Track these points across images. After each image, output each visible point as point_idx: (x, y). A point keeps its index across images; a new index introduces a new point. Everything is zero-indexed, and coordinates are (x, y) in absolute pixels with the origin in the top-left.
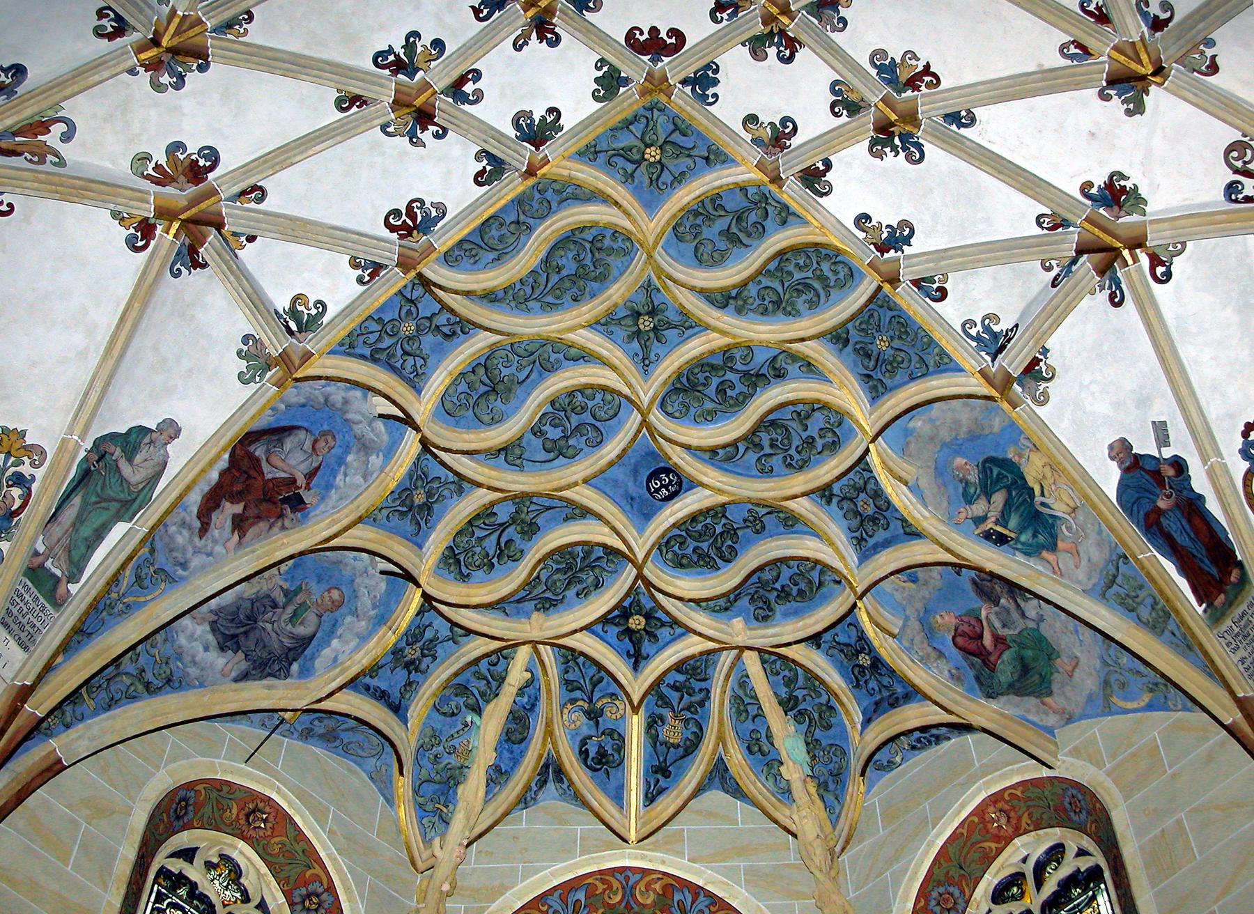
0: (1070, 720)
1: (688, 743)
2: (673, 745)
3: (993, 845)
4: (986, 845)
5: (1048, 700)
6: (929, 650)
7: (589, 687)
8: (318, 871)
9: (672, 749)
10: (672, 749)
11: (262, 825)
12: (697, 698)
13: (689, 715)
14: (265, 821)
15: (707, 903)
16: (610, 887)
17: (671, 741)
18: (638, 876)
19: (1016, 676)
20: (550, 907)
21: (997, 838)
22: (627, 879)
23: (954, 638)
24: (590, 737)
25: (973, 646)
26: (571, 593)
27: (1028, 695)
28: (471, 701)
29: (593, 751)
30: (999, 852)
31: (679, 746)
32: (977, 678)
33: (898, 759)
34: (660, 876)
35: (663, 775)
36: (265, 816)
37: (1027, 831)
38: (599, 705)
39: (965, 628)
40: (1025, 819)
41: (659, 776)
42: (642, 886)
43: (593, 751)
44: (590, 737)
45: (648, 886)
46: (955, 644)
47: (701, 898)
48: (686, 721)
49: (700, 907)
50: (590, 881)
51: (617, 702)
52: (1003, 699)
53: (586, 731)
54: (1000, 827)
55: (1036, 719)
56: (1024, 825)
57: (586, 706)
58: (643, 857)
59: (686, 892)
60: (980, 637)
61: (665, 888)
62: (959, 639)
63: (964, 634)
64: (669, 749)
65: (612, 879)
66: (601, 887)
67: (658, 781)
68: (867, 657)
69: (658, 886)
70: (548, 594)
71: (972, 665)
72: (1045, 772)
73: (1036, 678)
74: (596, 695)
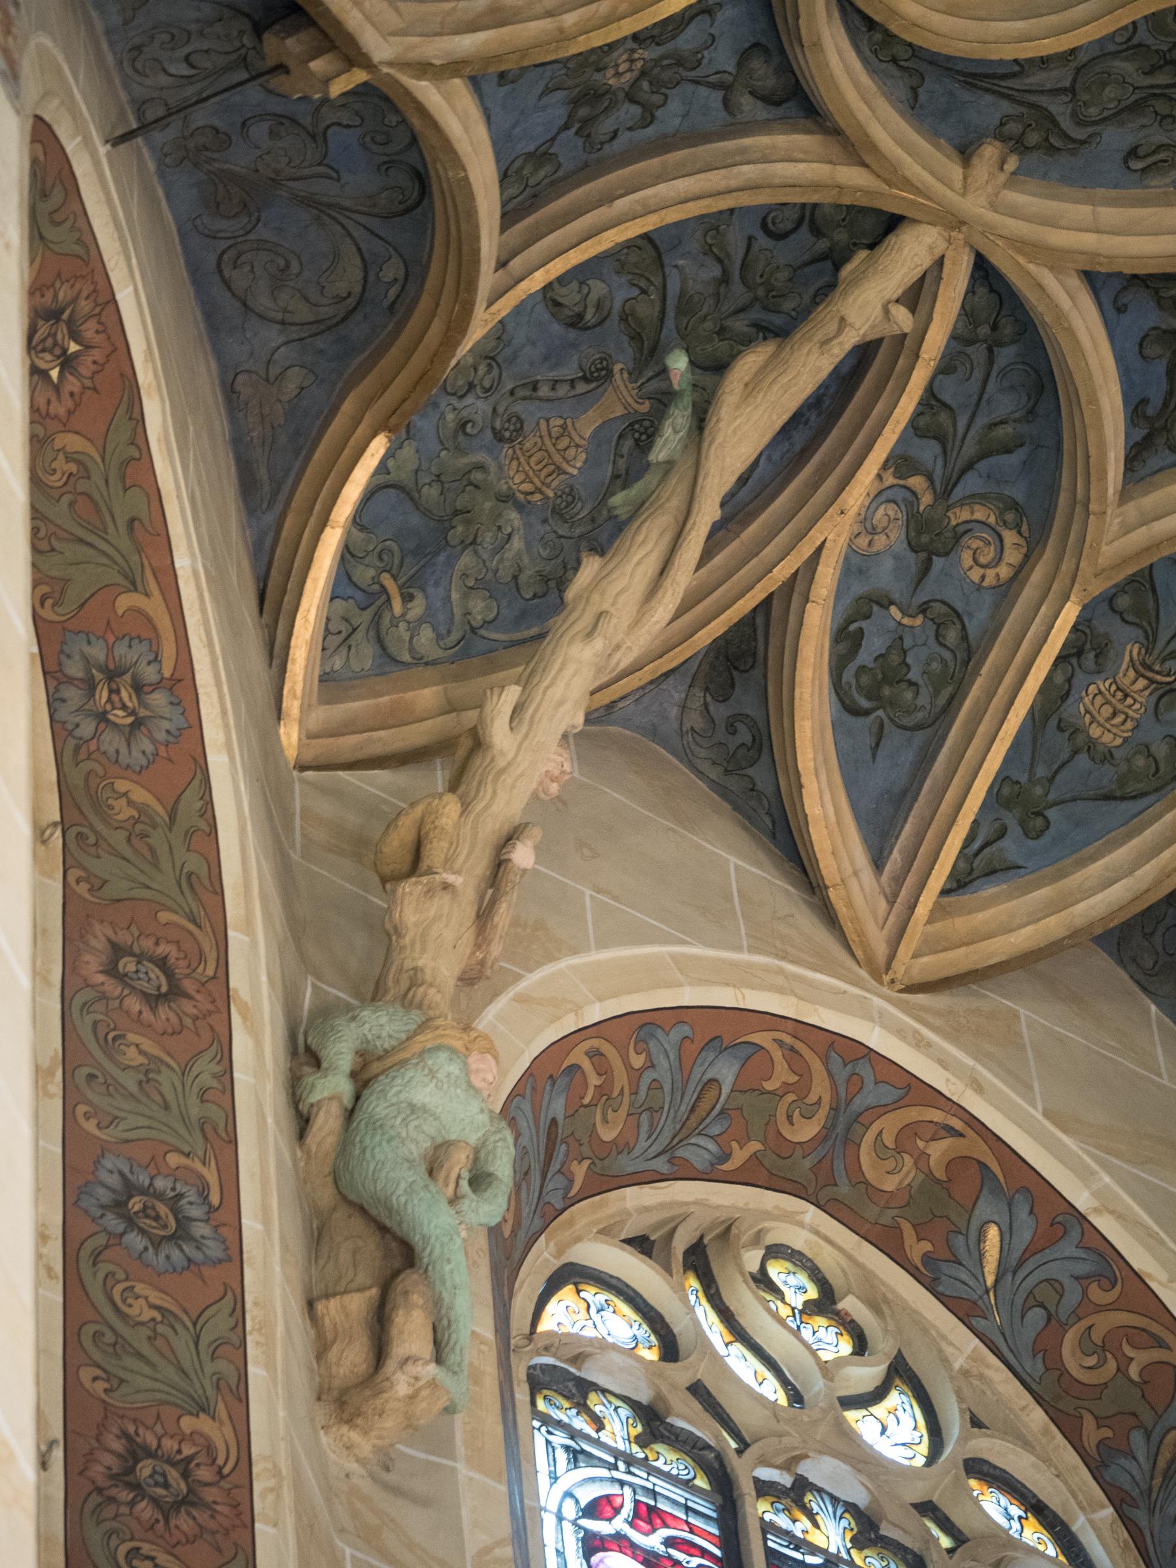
1: (1140, 761)
2: (1091, 746)
7: (970, 449)
8: (155, 606)
9: (1083, 760)
10: (1083, 760)
11: (54, 374)
15: (1082, 1268)
16: (802, 1087)
17: (1095, 731)
18: (887, 1094)
20: (651, 1065)
22: (855, 1083)
24: (885, 602)
26: (1116, 138)
28: (647, 310)
29: (874, 645)
31: (1108, 756)
35: (1022, 823)
36: (73, 347)
38: (961, 515)
41: (1011, 820)
42: (888, 1126)
43: (874, 645)
44: (885, 602)
45: (908, 1132)
47: (1068, 1248)
49: (1054, 1270)
51: (1010, 537)
53: (885, 577)
57: (926, 499)
58: (920, 1044)
59: (1023, 1212)
61: (955, 1164)
64: (1076, 752)
65: (817, 1065)
66: (782, 1075)
67: (1002, 833)
69: (938, 1151)
70: (1059, 108)
74: (971, 483)
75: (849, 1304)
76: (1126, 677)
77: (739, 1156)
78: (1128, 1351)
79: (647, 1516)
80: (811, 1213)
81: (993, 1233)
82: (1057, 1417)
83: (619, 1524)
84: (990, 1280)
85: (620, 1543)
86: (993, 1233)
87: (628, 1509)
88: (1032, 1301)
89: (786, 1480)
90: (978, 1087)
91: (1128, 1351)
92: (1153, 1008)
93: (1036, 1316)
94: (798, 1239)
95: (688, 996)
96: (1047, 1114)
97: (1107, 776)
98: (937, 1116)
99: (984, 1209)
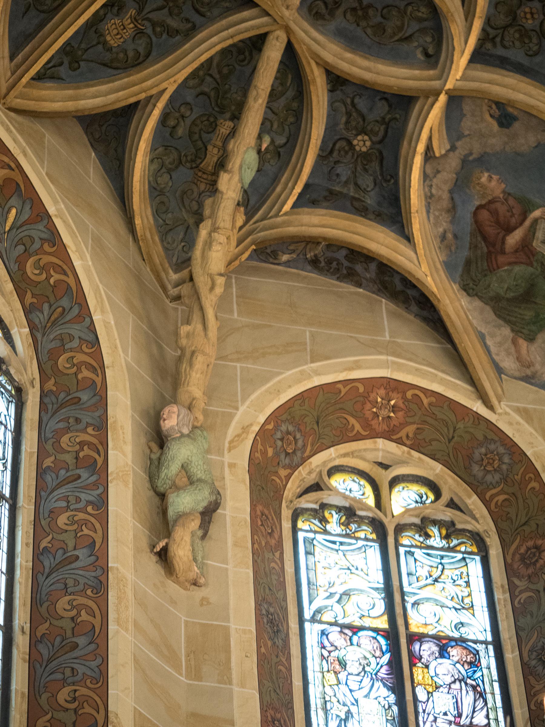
0: (528, 379)
1: (121, 55)
2: (105, 43)
3: (358, 427)
4: (352, 421)
5: (523, 344)
6: (446, 196)
9: (100, 47)
10: (100, 47)
12: (173, 23)
13: (149, 31)
15: (43, 236)
17: (108, 38)
19: (511, 295)
21: (366, 425)
23: (480, 207)
25: (491, 231)
27: (508, 322)
30: (358, 438)
32: (468, 263)
33: (285, 258)
34: (13, 165)
35: (70, 63)
37: (399, 442)
39: (502, 209)
40: (410, 429)
41: (66, 61)
46: (475, 214)
47: (41, 226)
48: (139, 33)
49: (33, 233)
52: (478, 303)
54: (376, 415)
55: (493, 349)
56: (402, 434)
59: (27, 207)
60: (509, 230)
62: (484, 215)
63: (495, 213)
64: (98, 43)
67: (61, 64)
68: (368, 143)
71: (474, 247)
72: (478, 407)
73: (529, 314)
76: (127, 21)
78: (52, 272)
81: (14, 211)
82: (17, 288)
84: (7, 229)
86: (14, 211)
88: (21, 242)
90: (25, 155)
91: (52, 272)
92: (93, 154)
93: (21, 248)
96: (47, 174)
97: (108, 56)
98: (6, 159)
99: (14, 201)
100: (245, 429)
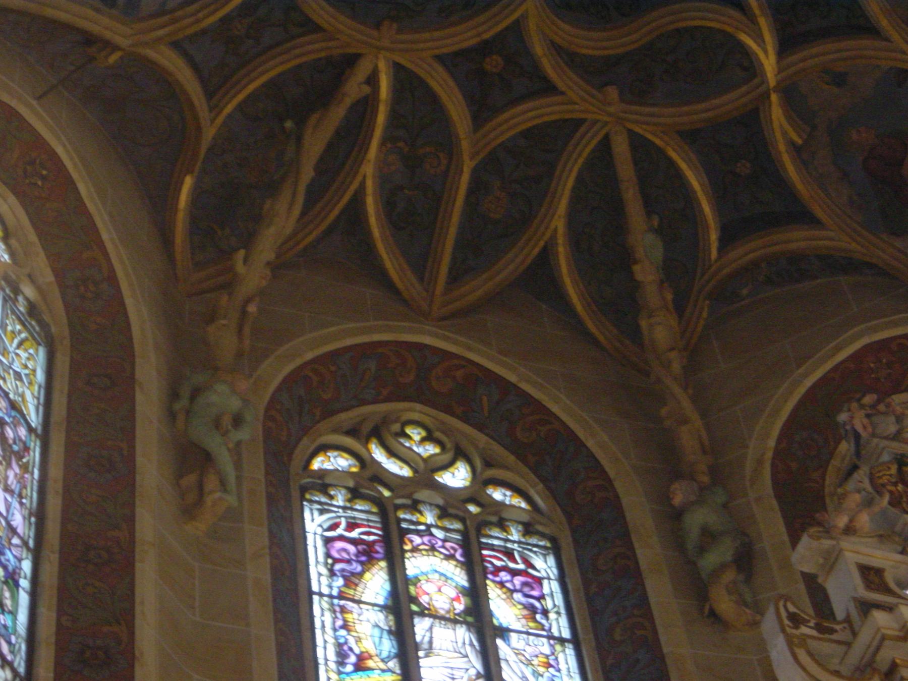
11: (40, 183)
14: (44, 178)
33: (745, 292)
34: (463, 363)
36: (44, 172)
50: (380, 350)
51: (441, 155)
57: (406, 149)
68: (748, 165)
69: (459, 374)
75: (437, 434)
77: (385, 392)
78: (539, 428)
79: (351, 527)
80: (418, 406)
81: (485, 399)
82: (518, 456)
83: (340, 531)
84: (487, 415)
85: (341, 538)
86: (485, 399)
87: (343, 524)
89: (407, 501)
90: (469, 349)
91: (539, 428)
92: (544, 306)
94: (415, 416)
95: (349, 342)
96: (500, 353)
98: (456, 362)
100: (760, 462)
